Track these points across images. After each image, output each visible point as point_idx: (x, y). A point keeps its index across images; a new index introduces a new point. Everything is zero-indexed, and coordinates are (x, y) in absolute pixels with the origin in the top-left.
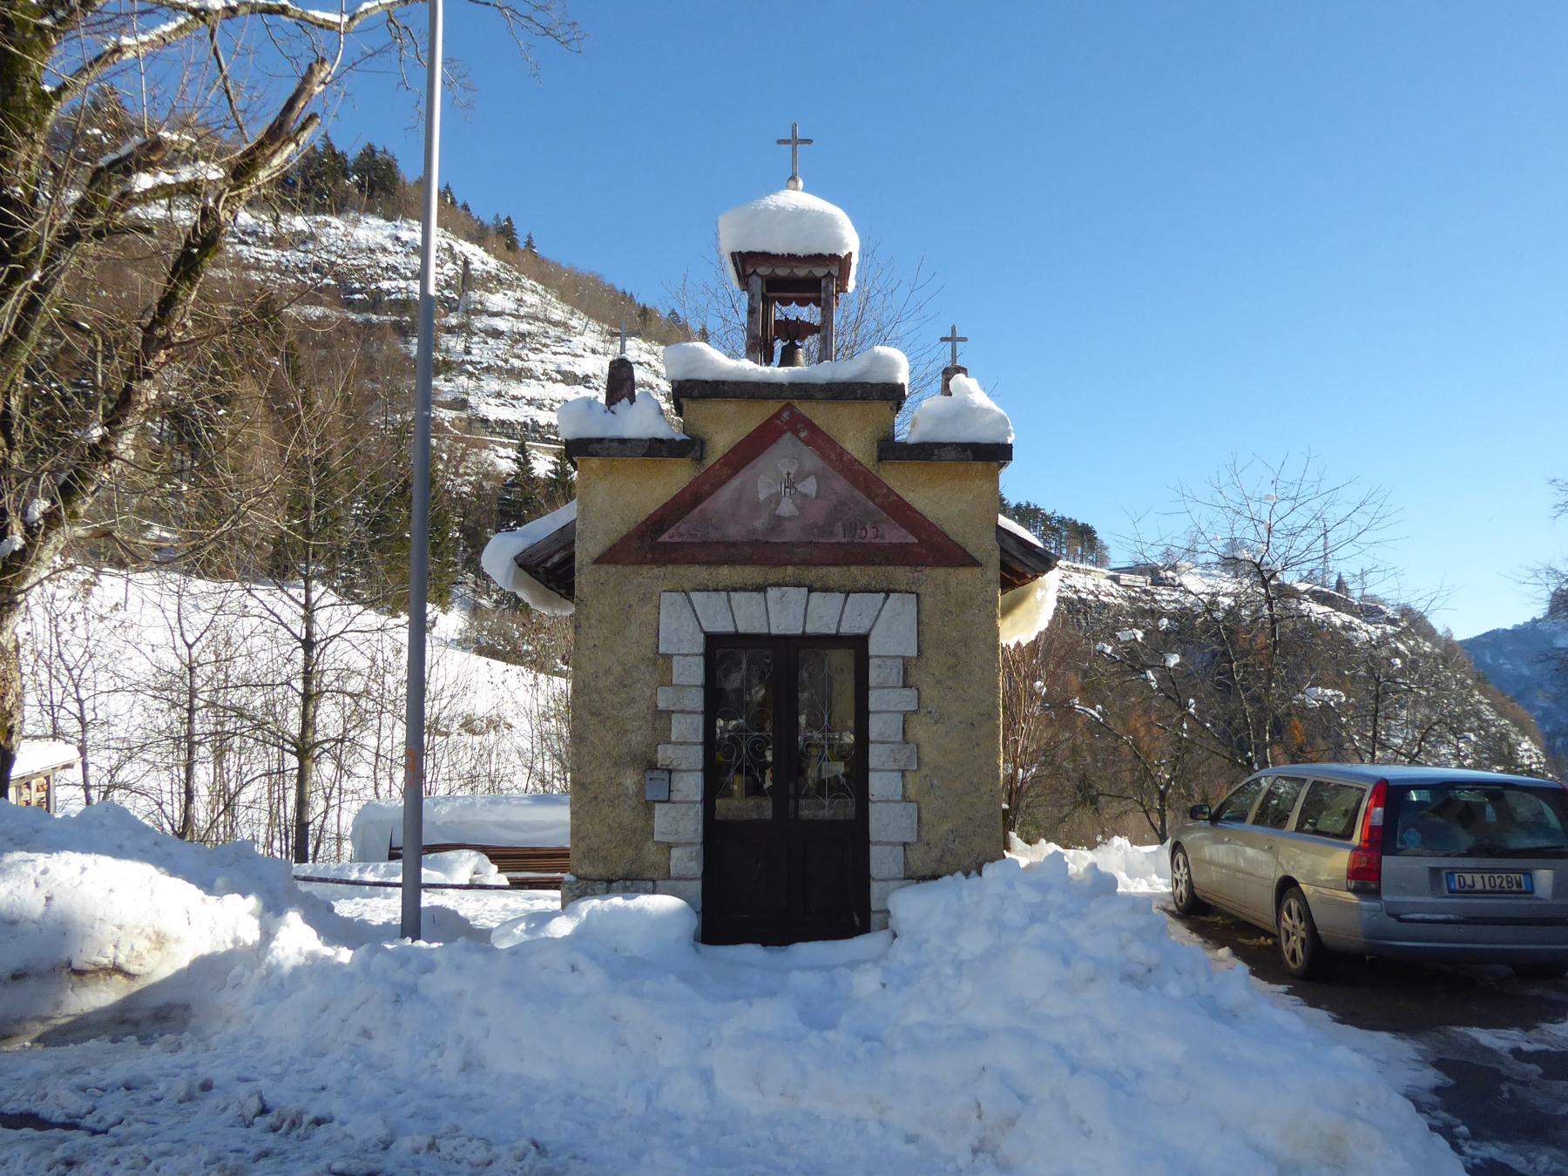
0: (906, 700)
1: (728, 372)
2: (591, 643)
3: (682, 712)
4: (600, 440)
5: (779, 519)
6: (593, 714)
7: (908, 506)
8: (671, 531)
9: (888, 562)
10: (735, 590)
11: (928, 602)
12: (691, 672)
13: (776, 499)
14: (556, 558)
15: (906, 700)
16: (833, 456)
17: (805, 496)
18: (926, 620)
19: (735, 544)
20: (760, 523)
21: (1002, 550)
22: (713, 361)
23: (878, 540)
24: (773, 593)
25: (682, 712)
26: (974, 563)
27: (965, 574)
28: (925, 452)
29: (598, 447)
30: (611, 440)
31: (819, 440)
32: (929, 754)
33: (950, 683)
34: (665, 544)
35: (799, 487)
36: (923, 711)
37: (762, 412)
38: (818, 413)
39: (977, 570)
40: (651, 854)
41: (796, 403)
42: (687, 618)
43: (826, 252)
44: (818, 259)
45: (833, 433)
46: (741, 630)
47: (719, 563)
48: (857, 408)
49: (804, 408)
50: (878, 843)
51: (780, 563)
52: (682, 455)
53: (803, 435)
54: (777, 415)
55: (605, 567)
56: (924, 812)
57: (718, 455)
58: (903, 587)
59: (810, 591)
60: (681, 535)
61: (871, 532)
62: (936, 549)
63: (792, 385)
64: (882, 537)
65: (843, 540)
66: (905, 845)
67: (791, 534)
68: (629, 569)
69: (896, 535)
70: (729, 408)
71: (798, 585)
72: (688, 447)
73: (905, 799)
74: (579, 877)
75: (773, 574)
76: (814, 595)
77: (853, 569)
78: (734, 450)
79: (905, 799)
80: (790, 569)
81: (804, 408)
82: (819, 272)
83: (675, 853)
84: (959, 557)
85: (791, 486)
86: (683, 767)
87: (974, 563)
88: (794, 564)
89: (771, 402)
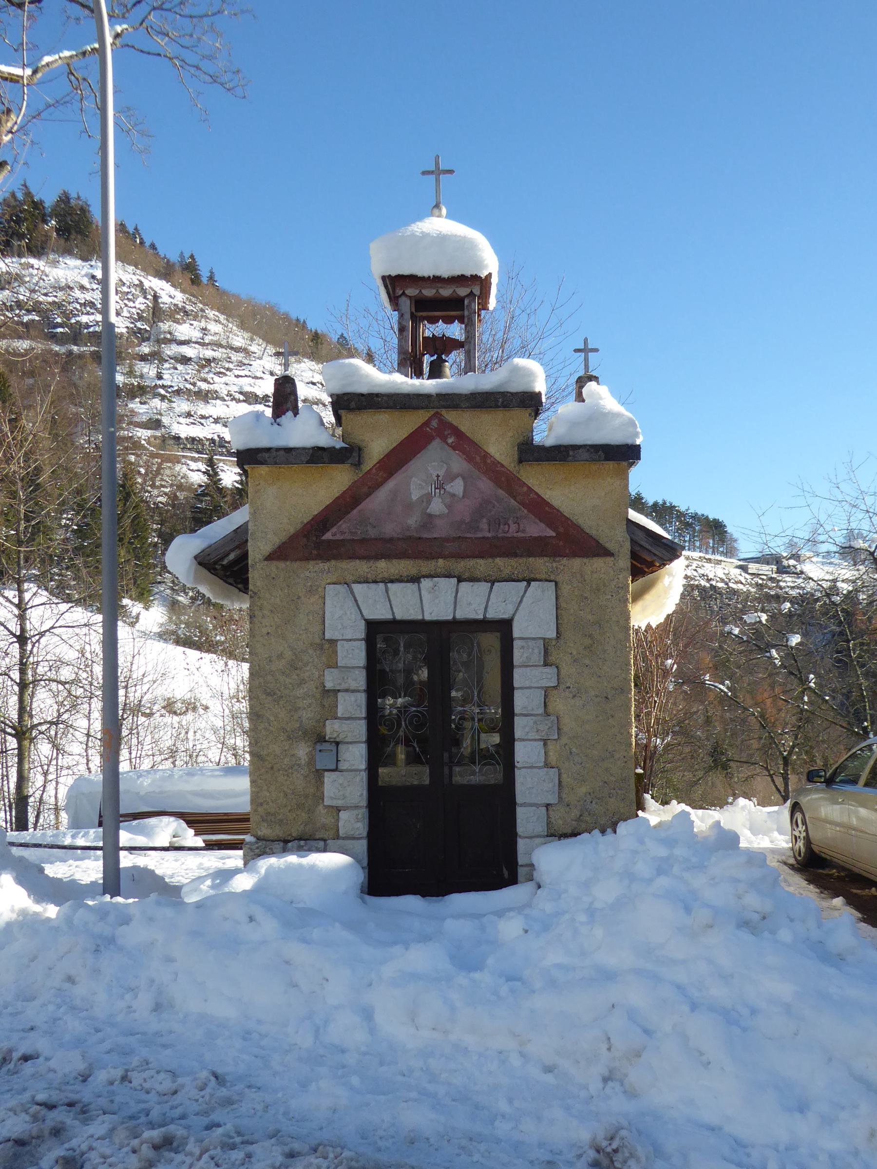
0: (547, 677)
1: (381, 386)
2: (265, 630)
3: (347, 691)
4: (268, 450)
5: (430, 516)
6: (268, 694)
7: (548, 504)
8: (334, 529)
9: (530, 554)
10: (392, 581)
11: (565, 589)
12: (354, 655)
13: (428, 498)
14: (232, 556)
15: (547, 677)
16: (478, 459)
17: (453, 495)
18: (563, 605)
19: (391, 540)
20: (413, 521)
21: (632, 540)
22: (367, 376)
23: (520, 535)
24: (426, 583)
25: (347, 691)
26: (603, 552)
27: (599, 563)
28: (561, 454)
29: (267, 455)
30: (278, 449)
31: (465, 445)
32: (568, 723)
33: (587, 662)
34: (329, 542)
35: (448, 487)
36: (562, 687)
37: (412, 421)
39: (609, 560)
40: (323, 817)
41: (444, 412)
42: (348, 607)
43: (468, 273)
44: (461, 280)
45: (477, 438)
46: (399, 617)
47: (377, 557)
48: (499, 415)
49: (451, 416)
50: (524, 805)
52: (342, 462)
53: (450, 441)
54: (426, 424)
55: (275, 563)
56: (564, 776)
57: (374, 461)
58: (543, 576)
59: (459, 581)
60: (342, 533)
61: (513, 527)
62: (571, 541)
63: (437, 395)
64: (524, 531)
65: (489, 535)
66: (548, 806)
67: (442, 530)
68: (297, 564)
69: (535, 529)
70: (383, 417)
71: (449, 576)
72: (346, 454)
73: (547, 765)
74: (259, 839)
75: (427, 566)
76: (463, 585)
77: (498, 560)
78: (388, 456)
79: (547, 765)
80: (440, 560)
81: (451, 416)
82: (462, 292)
83: (343, 815)
84: (593, 549)
85: (440, 486)
86: (349, 740)
87: (603, 552)
88: (444, 557)
89: (421, 412)
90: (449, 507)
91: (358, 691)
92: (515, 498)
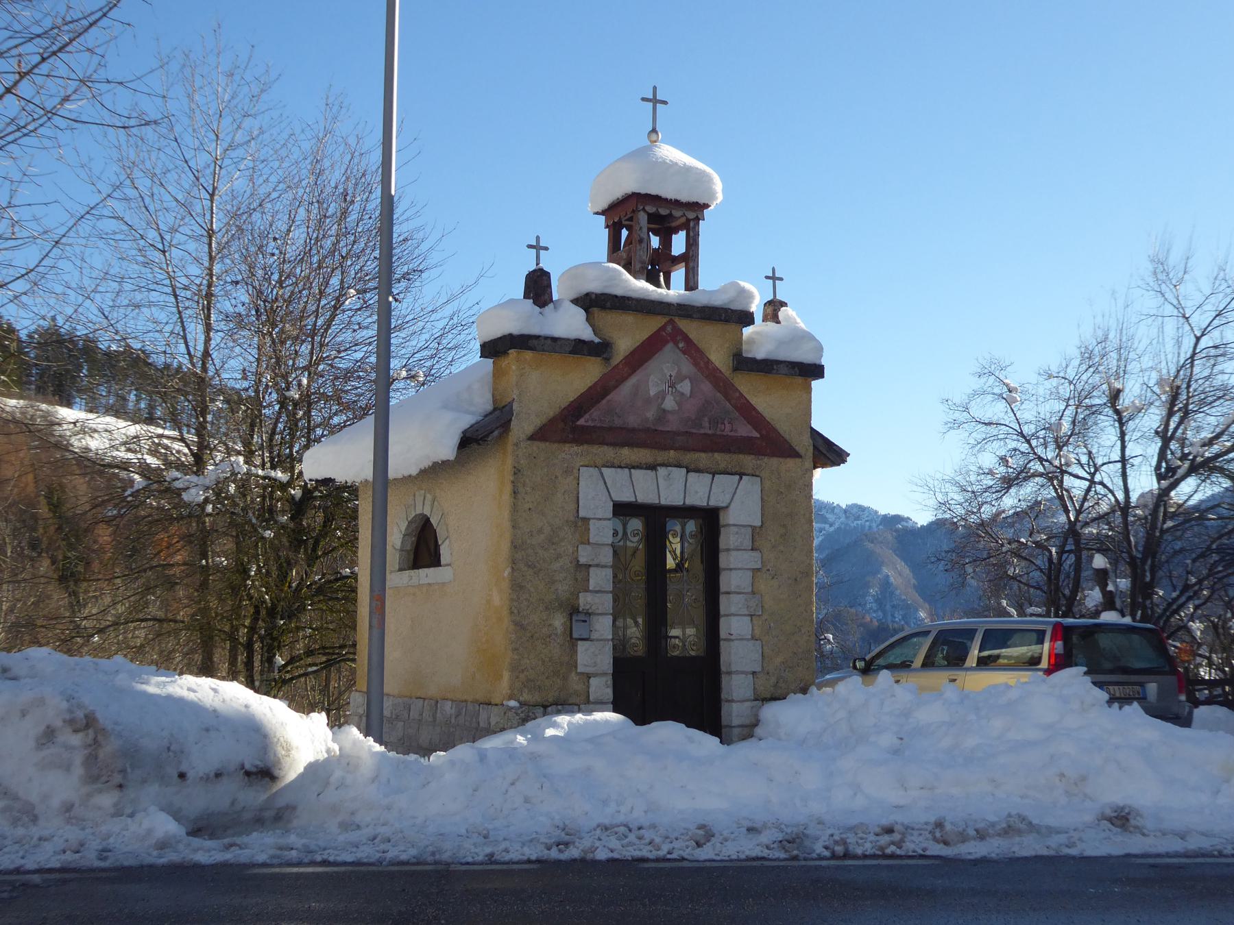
0: (751, 560)
2: (527, 506)
3: (597, 566)
5: (664, 410)
6: (529, 566)
7: (755, 409)
8: (587, 416)
9: (741, 452)
10: (634, 468)
12: (603, 531)
15: (751, 560)
16: (702, 364)
19: (633, 430)
20: (651, 414)
21: (815, 447)
23: (732, 434)
24: (662, 471)
25: (597, 566)
26: (797, 455)
27: (790, 463)
28: (766, 367)
31: (692, 350)
33: (782, 548)
34: (583, 427)
35: (678, 387)
37: (653, 324)
38: (692, 329)
39: (798, 460)
40: (575, 683)
41: (676, 319)
42: (601, 487)
45: (702, 345)
46: (639, 501)
47: (623, 445)
49: (684, 324)
51: (665, 448)
52: (597, 355)
53: (681, 345)
54: (663, 328)
55: (537, 443)
60: (593, 420)
61: (728, 427)
67: (673, 425)
70: (629, 319)
71: (679, 466)
72: (598, 349)
74: (522, 704)
75: (662, 456)
77: (716, 455)
78: (633, 353)
80: (672, 452)
81: (683, 324)
84: (790, 452)
85: (672, 386)
87: (797, 455)
88: (676, 449)
89: (659, 317)
90: (679, 404)
91: (606, 567)
92: (729, 401)
